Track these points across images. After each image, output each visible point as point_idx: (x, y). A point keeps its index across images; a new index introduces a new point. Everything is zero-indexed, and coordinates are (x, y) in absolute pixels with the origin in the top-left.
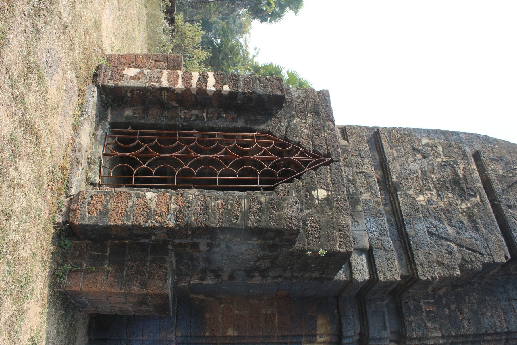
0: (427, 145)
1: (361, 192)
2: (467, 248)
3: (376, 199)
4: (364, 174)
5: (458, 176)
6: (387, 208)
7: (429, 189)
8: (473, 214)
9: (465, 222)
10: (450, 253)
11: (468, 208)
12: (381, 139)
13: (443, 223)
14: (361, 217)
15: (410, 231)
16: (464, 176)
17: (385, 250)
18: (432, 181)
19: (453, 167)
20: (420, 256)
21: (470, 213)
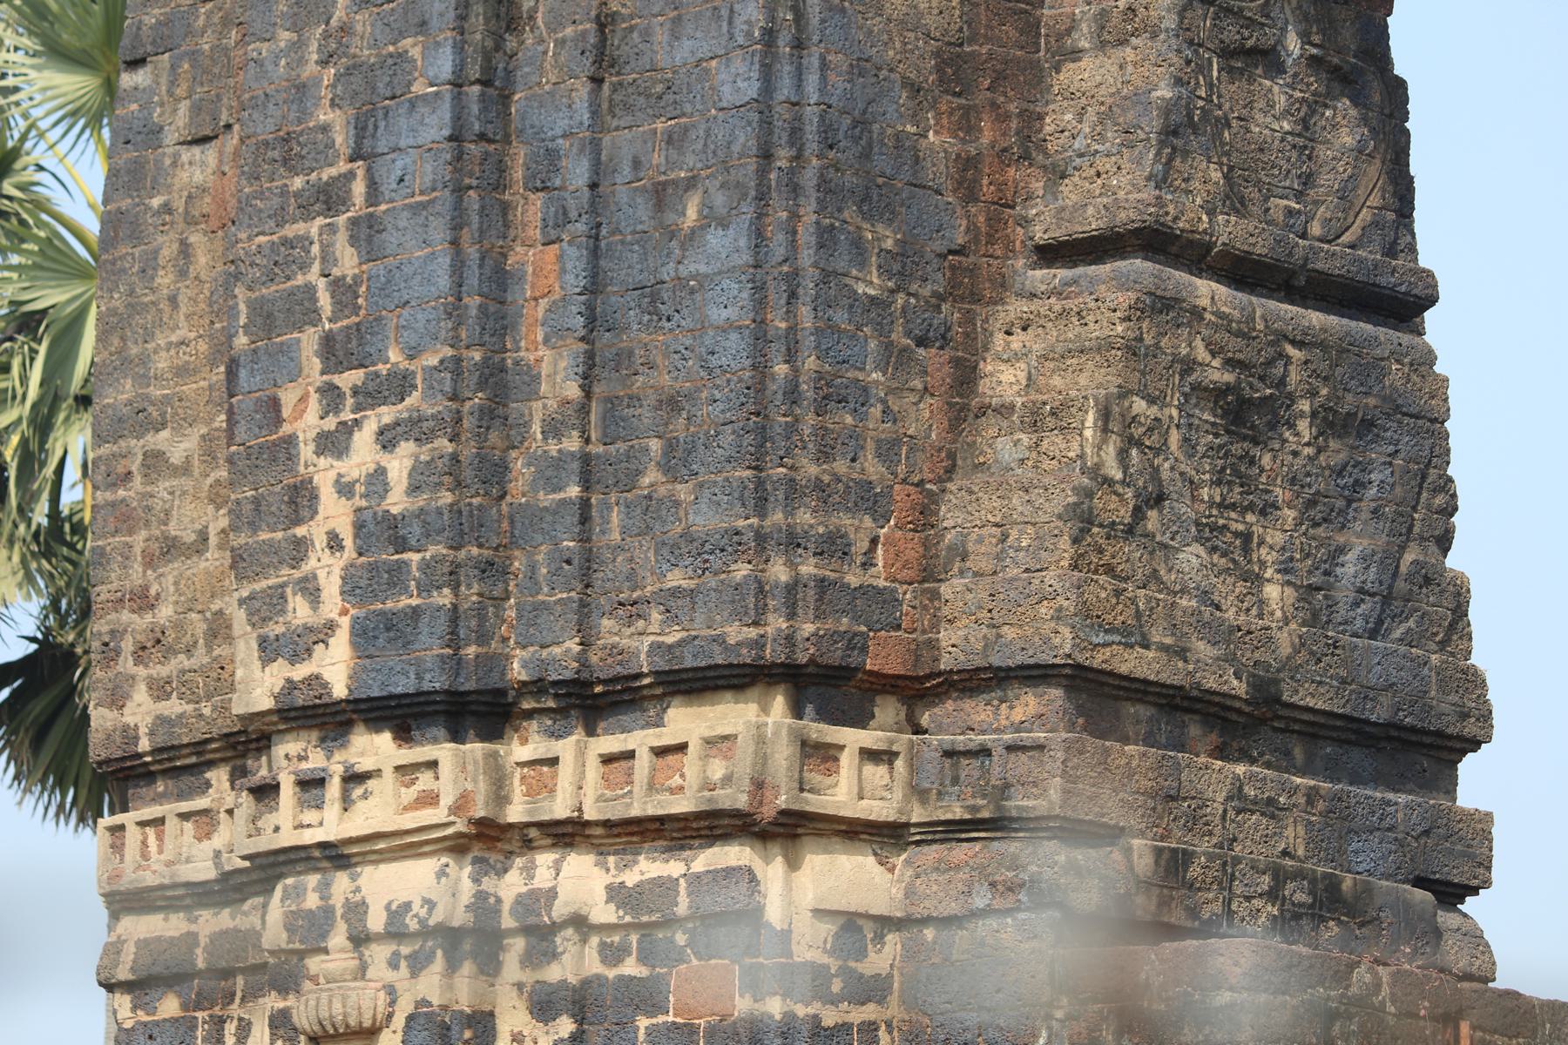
0: (1123, 455)
1: (1285, 853)
2: (1414, 509)
3: (1302, 800)
4: (1231, 814)
5: (1229, 389)
6: (1298, 753)
7: (1246, 537)
8: (1331, 409)
9: (1343, 456)
10: (1427, 581)
11: (1314, 414)
12: (1111, 674)
13: (1341, 550)
14: (1368, 889)
15: (1379, 713)
16: (1230, 363)
17: (1426, 833)
18: (1220, 506)
19: (1196, 387)
20: (1444, 707)
21: (1325, 419)
